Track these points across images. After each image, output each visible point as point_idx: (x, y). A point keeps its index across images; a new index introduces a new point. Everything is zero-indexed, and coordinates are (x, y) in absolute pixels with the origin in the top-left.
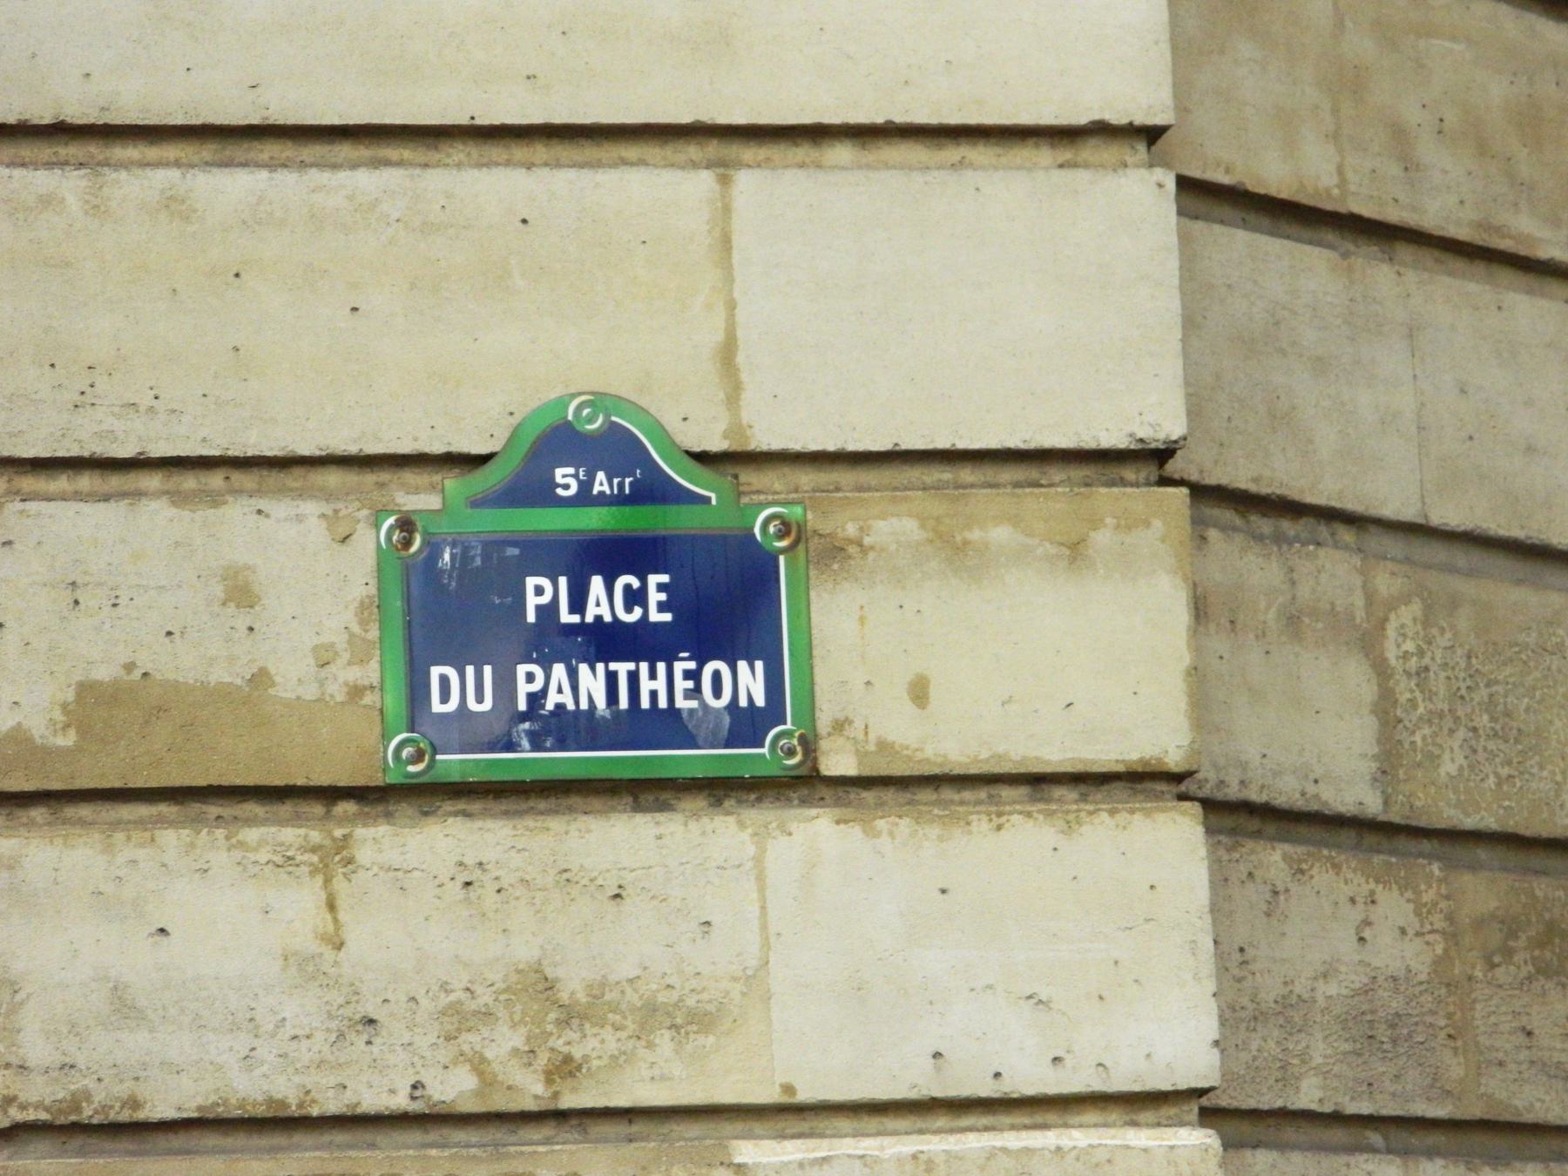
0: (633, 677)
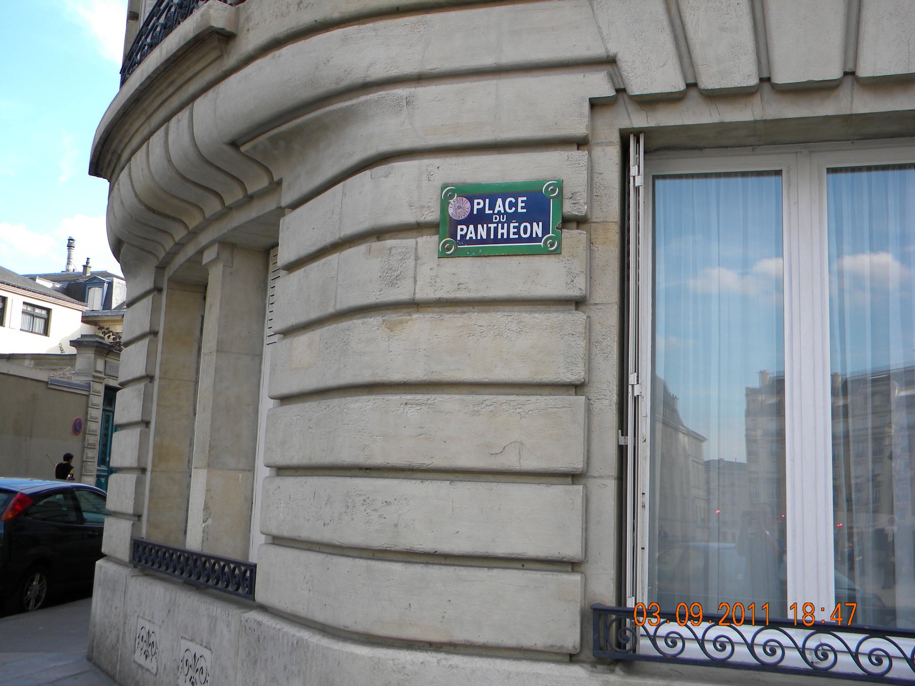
0: (496, 229)
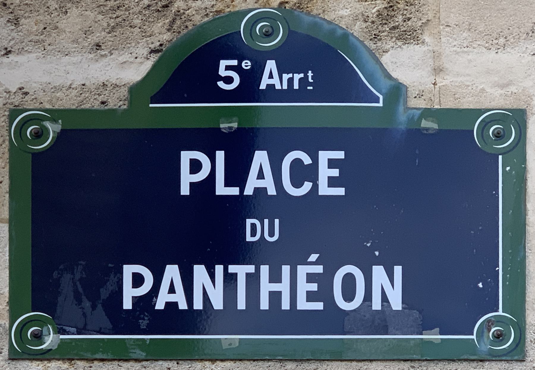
0: (253, 280)
